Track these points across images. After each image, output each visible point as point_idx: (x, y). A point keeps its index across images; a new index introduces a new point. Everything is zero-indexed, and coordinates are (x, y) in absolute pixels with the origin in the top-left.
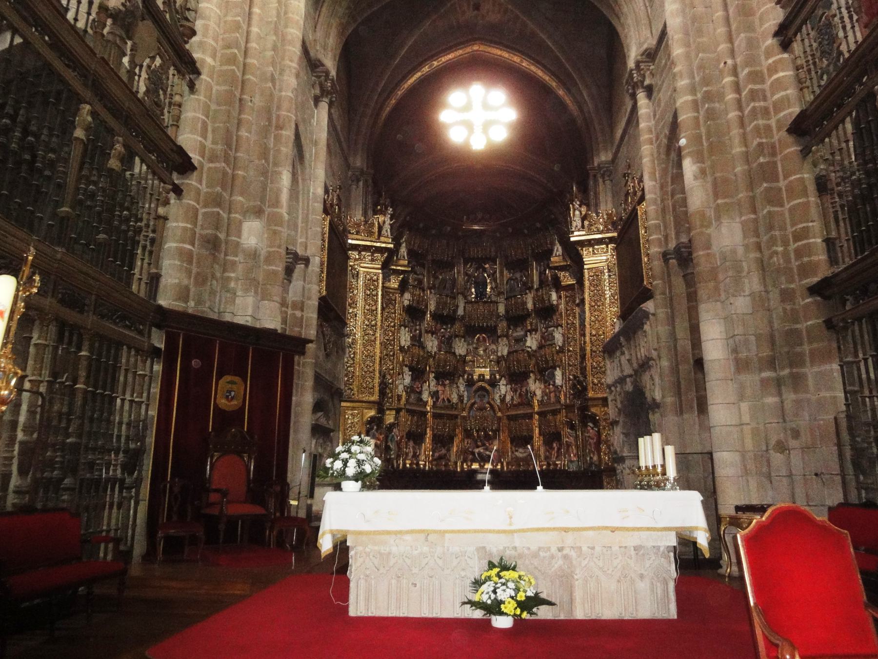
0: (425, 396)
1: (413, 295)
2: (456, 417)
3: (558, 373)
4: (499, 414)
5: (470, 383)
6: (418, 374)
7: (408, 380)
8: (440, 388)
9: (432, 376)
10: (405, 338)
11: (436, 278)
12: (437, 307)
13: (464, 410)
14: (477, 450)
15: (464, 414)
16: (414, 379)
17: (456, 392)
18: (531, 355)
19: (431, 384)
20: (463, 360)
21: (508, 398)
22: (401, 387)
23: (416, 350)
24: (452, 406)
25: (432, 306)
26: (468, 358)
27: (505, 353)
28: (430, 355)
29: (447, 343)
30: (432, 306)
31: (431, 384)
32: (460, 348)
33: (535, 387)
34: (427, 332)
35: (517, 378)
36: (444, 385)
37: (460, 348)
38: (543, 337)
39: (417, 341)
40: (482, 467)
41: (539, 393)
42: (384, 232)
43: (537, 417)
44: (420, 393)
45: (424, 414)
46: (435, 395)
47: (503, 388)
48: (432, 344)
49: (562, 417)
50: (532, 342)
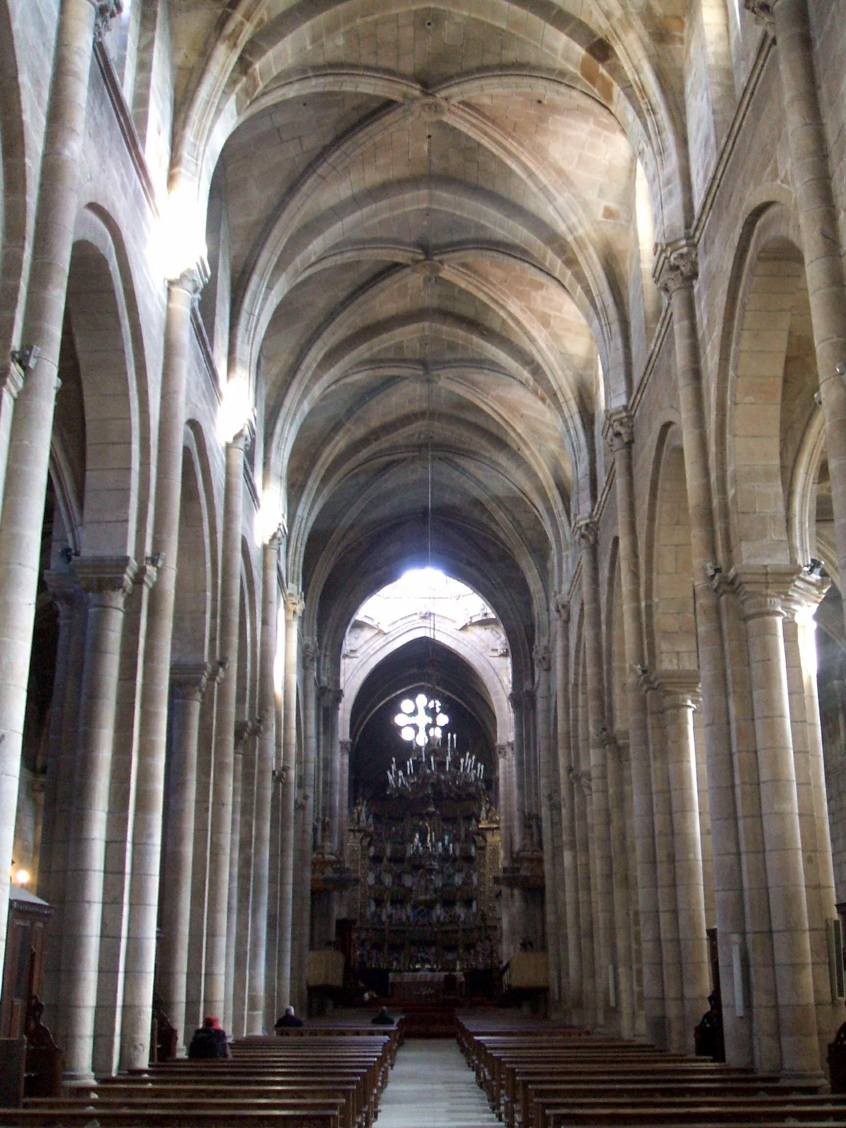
0: (384, 918)
1: (376, 847)
2: (404, 932)
3: (474, 904)
4: (435, 929)
5: (414, 907)
6: (379, 903)
7: (373, 908)
8: (394, 911)
9: (388, 904)
10: (371, 879)
11: (390, 829)
12: (392, 852)
13: (410, 926)
14: (419, 955)
15: (411, 929)
16: (377, 906)
17: (407, 912)
18: (459, 889)
19: (388, 909)
20: (410, 890)
21: (442, 918)
22: (368, 914)
23: (377, 886)
24: (402, 924)
25: (388, 852)
26: (414, 888)
27: (441, 885)
28: (387, 889)
29: (398, 877)
30: (388, 852)
31: (388, 909)
32: (408, 881)
33: (460, 911)
34: (385, 871)
35: (448, 903)
36: (396, 908)
37: (408, 881)
38: (466, 876)
39: (379, 880)
40: (423, 966)
41: (462, 915)
42: (361, 819)
43: (461, 932)
44: (380, 916)
45: (383, 931)
46: (390, 917)
47: (439, 911)
48: (388, 880)
49: (476, 934)
50: (458, 880)
